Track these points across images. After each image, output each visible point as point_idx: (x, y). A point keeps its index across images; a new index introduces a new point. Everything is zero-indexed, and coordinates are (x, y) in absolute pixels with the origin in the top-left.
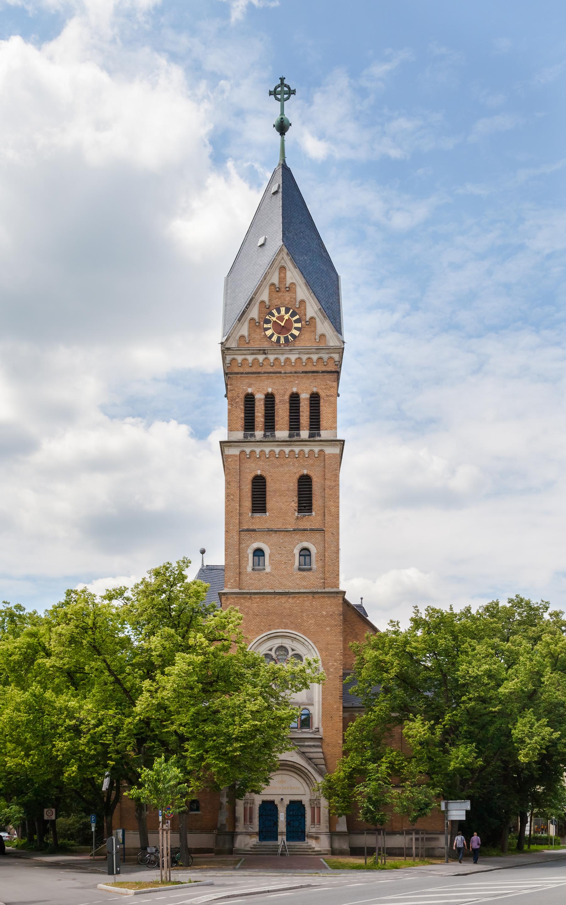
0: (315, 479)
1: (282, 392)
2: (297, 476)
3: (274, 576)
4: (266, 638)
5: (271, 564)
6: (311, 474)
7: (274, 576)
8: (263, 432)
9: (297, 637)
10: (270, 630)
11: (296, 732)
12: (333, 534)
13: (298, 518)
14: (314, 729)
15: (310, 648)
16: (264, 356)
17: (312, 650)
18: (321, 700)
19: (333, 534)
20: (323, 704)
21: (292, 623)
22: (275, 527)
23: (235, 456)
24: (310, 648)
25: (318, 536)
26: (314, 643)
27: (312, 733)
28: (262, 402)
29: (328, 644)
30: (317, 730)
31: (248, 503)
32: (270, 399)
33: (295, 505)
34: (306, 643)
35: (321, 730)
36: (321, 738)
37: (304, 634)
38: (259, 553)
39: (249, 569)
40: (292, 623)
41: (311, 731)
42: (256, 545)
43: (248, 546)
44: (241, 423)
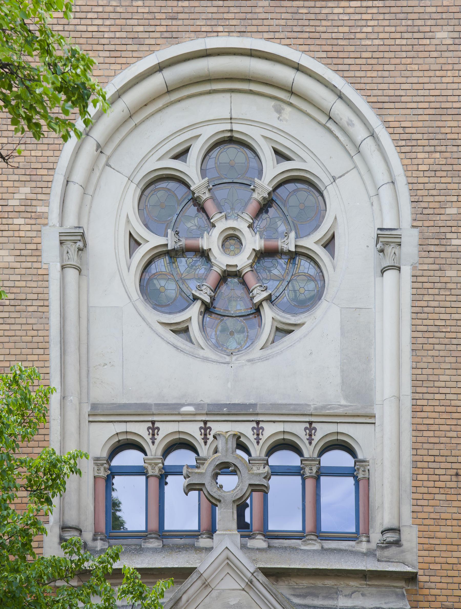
4: (156, 82)
9: (303, 82)
10: (173, 37)
11: (295, 549)
14: (376, 537)
15: (359, 133)
17: (368, 146)
18: (407, 389)
20: (416, 409)
24: (359, 133)
26: (378, 105)
27: (370, 554)
29: (441, 112)
30: (391, 537)
34: (340, 110)
35: (410, 537)
36: (411, 578)
37: (330, 60)
41: (364, 547)
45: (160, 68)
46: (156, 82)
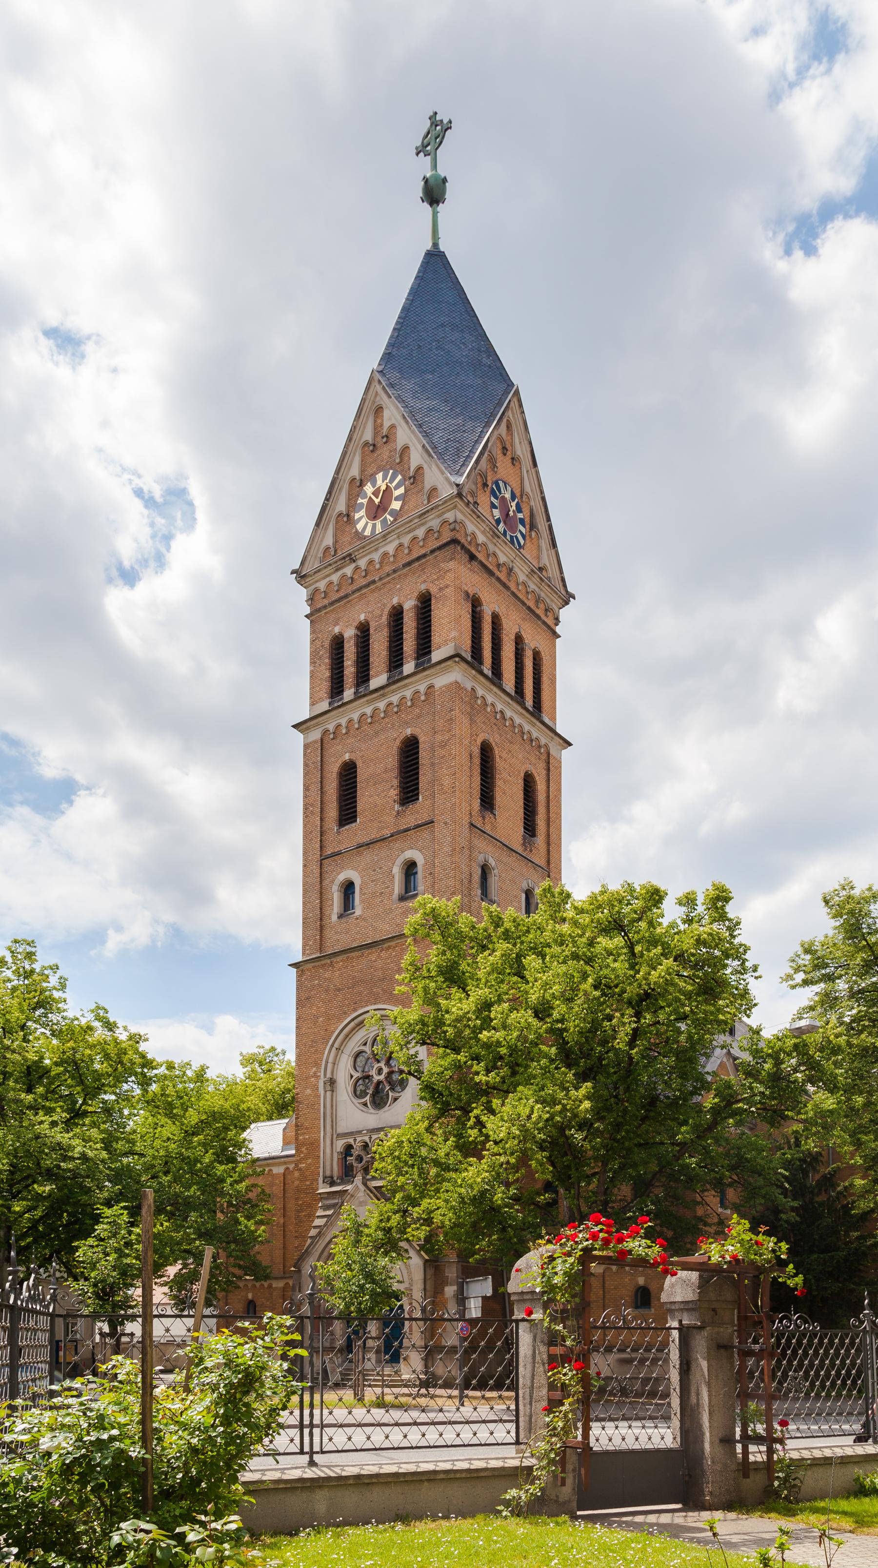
0: (422, 739)
1: (378, 612)
2: (398, 743)
3: (365, 919)
4: (352, 1024)
5: (362, 901)
6: (417, 732)
7: (365, 919)
8: (353, 690)
10: (355, 1010)
12: (446, 823)
13: (398, 812)
16: (353, 565)
19: (446, 823)
21: (384, 991)
22: (366, 839)
23: (315, 742)
25: (425, 834)
28: (352, 642)
31: (333, 812)
32: (364, 631)
33: (394, 793)
38: (348, 888)
39: (334, 918)
40: (384, 991)
42: (342, 877)
43: (333, 882)
44: (325, 686)
45: (353, 1020)
46: (352, 1024)
